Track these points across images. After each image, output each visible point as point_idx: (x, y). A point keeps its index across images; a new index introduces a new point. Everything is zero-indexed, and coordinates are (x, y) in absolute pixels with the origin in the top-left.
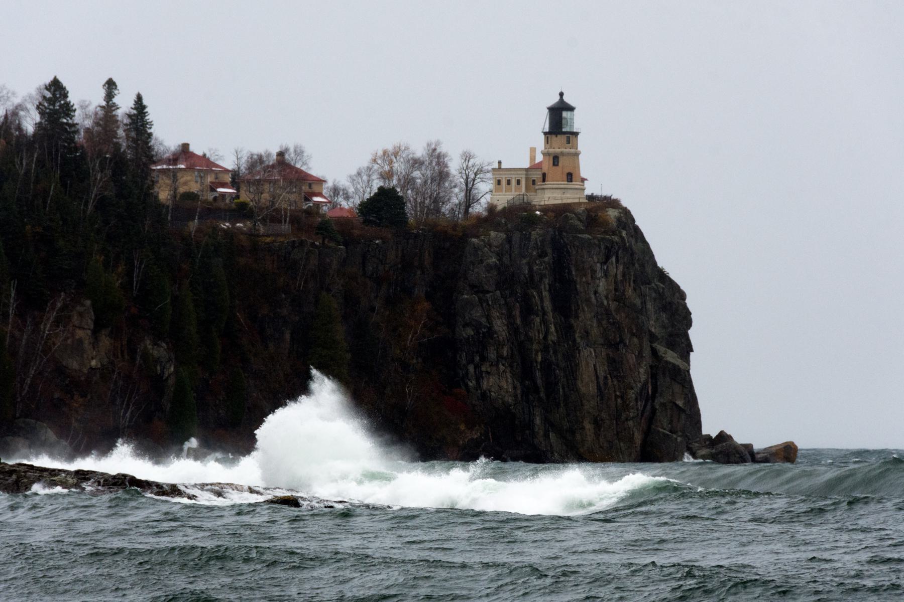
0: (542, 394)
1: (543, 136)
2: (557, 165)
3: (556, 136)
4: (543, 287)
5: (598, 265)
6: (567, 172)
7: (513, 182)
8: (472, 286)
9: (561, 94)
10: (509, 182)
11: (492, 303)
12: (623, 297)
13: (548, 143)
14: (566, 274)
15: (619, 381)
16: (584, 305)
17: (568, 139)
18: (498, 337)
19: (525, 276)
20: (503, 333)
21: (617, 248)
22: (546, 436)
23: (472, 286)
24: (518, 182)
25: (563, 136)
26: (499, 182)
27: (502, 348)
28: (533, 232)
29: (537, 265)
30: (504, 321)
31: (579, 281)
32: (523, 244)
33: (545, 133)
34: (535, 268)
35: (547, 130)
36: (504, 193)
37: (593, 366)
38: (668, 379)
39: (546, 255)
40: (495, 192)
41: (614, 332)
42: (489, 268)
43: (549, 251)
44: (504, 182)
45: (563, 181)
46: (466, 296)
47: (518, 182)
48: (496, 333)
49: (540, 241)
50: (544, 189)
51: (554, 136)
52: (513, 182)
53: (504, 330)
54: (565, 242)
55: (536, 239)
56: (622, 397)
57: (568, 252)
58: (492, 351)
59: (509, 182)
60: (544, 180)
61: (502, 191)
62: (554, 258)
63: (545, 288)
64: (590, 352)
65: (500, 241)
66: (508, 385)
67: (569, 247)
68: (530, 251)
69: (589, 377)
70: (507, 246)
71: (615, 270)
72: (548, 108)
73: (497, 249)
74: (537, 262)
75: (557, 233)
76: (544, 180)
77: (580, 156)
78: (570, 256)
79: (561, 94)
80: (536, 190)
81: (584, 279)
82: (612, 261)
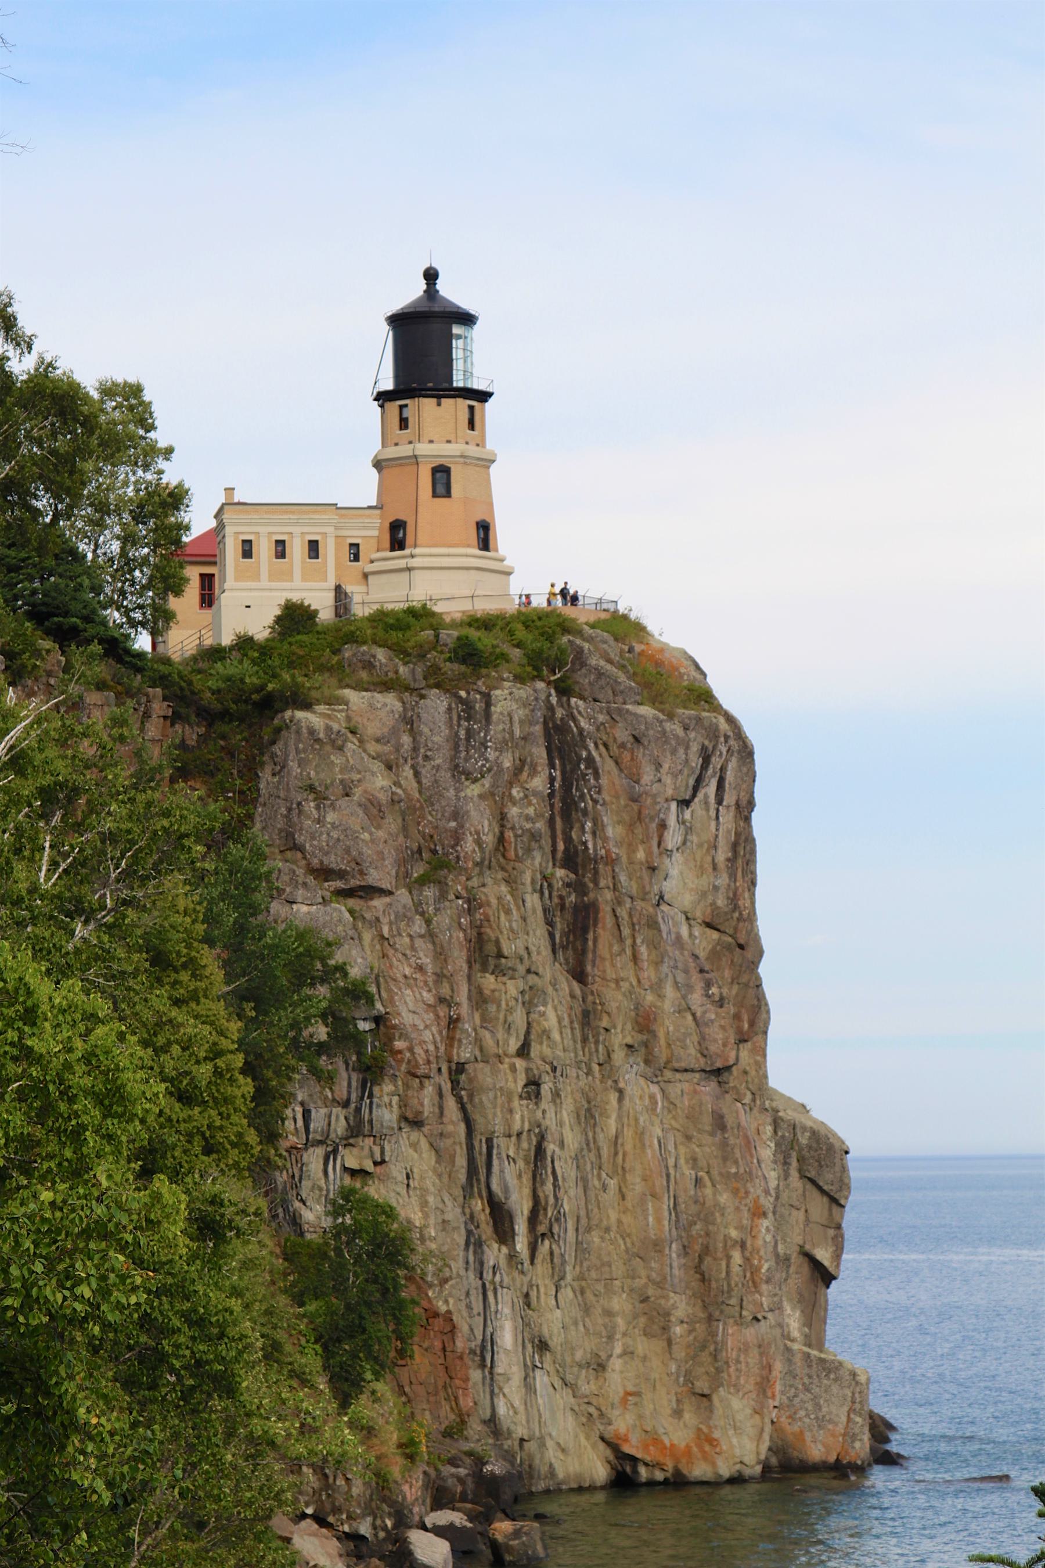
0: (521, 1245)
1: (375, 408)
2: (448, 494)
3: (439, 404)
4: (527, 878)
5: (674, 806)
6: (479, 518)
7: (297, 550)
8: (324, 873)
9: (431, 276)
10: (281, 549)
11: (391, 930)
12: (736, 915)
13: (404, 423)
14: (588, 837)
15: (735, 1192)
16: (639, 941)
17: (471, 408)
18: (411, 1049)
19: (478, 842)
20: (427, 1036)
21: (724, 750)
22: (529, 1386)
23: (324, 873)
24: (314, 548)
25: (460, 401)
26: (247, 550)
27: (422, 1086)
28: (498, 692)
29: (514, 804)
30: (425, 994)
31: (624, 859)
32: (462, 734)
33: (382, 398)
34: (514, 811)
35: (388, 384)
36: (265, 583)
37: (656, 1142)
38: (794, 1174)
39: (534, 772)
40: (237, 579)
41: (723, 1028)
42: (374, 810)
43: (539, 753)
44: (264, 550)
45: (469, 546)
46: (305, 909)
47: (314, 548)
48: (404, 1036)
49: (521, 722)
50: (409, 569)
51: (428, 404)
52: (297, 550)
53: (426, 1027)
54: (581, 731)
55: (510, 716)
56: (743, 1245)
57: (590, 761)
58: (386, 1099)
59: (281, 549)
60: (397, 543)
61: (257, 577)
62: (552, 780)
63: (533, 882)
64: (652, 1097)
65: (390, 723)
66: (426, 1216)
67: (592, 746)
68: (491, 754)
69: (645, 1179)
70: (406, 739)
71: (713, 824)
72: (399, 321)
73: (387, 748)
74: (514, 792)
75: (554, 700)
76: (397, 543)
77: (494, 469)
78: (597, 775)
79: (431, 276)
80: (366, 576)
81: (641, 855)
82: (706, 796)
